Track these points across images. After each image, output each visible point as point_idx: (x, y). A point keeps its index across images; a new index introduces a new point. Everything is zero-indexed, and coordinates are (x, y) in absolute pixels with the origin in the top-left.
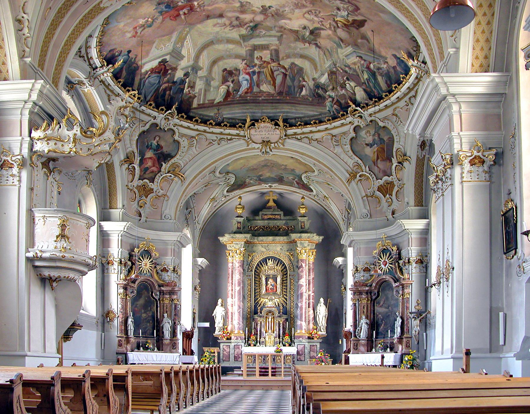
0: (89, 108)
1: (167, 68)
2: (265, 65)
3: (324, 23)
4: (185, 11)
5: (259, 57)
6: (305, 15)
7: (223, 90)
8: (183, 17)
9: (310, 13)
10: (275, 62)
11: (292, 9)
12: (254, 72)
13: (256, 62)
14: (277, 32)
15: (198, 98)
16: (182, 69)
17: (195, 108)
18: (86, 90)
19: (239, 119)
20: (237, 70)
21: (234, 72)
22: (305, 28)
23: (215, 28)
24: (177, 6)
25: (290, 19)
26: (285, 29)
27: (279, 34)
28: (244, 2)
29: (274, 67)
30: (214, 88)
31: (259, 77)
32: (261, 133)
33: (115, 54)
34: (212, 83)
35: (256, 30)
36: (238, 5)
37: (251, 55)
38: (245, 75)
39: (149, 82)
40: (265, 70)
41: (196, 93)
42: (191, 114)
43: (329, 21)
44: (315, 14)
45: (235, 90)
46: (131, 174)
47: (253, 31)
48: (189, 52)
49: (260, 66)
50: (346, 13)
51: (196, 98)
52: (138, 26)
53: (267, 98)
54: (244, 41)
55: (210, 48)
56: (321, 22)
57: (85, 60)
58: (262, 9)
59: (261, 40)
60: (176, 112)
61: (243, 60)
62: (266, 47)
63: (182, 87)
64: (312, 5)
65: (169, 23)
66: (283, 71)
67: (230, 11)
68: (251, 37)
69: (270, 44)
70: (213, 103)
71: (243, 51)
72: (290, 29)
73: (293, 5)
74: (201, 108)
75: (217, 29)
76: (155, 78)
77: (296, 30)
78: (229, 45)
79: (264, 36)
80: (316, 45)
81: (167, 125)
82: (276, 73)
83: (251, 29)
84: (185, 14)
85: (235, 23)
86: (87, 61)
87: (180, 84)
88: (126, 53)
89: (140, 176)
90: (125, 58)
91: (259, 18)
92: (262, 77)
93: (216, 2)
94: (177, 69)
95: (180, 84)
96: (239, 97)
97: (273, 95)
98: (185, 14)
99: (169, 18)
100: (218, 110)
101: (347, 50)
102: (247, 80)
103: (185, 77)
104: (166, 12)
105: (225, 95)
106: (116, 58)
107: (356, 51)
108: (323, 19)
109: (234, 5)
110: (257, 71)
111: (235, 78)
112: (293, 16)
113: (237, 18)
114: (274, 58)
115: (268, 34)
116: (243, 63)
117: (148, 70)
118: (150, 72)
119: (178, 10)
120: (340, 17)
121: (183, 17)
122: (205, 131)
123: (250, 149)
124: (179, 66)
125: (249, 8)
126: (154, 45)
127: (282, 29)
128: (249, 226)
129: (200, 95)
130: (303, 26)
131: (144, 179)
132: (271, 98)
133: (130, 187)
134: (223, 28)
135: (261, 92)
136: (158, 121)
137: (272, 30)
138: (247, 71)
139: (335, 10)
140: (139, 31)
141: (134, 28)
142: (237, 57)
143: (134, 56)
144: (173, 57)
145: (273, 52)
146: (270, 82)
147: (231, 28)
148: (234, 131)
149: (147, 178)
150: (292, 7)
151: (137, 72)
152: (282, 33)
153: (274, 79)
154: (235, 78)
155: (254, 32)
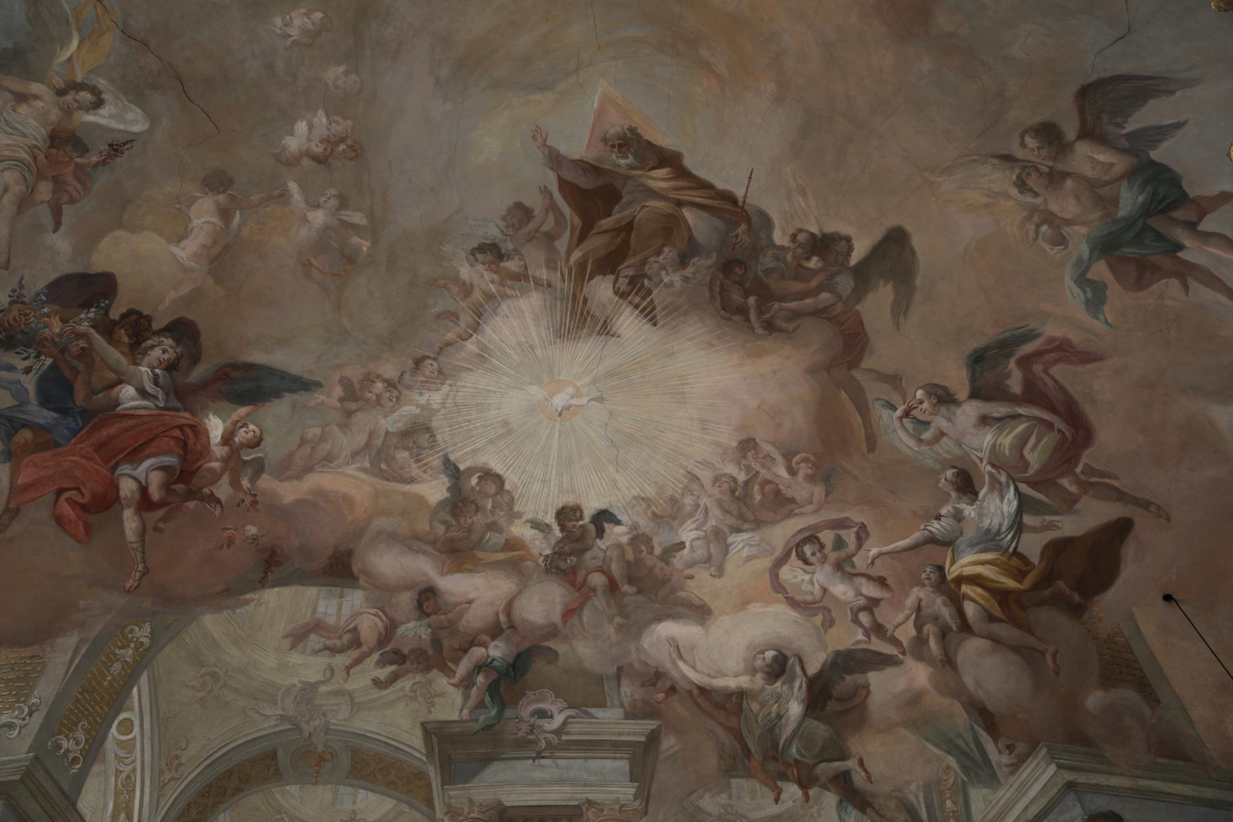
3: (883, 615)
6: (786, 573)
8: (130, 521)
9: (808, 550)
14: (631, 715)
22: (779, 668)
23: (295, 658)
24: (111, 410)
25: (701, 613)
26: (673, 689)
27: (637, 730)
28: (471, 471)
35: (515, 703)
36: (435, 490)
43: (916, 593)
44: (833, 556)
47: (503, 706)
50: (1009, 504)
54: (451, 775)
55: (254, 800)
56: (871, 605)
58: (558, 533)
64: (819, 491)
69: (589, 802)
72: (703, 690)
73: (720, 503)
78: (362, 793)
79: (562, 746)
80: (844, 785)
83: (493, 689)
84: (145, 503)
85: (414, 631)
101: (1022, 790)
107: (1081, 778)
108: (881, 582)
112: (718, 583)
113: (427, 597)
115: (579, 730)
120: (972, 545)
121: (130, 521)
125: (493, 527)
130: (770, 654)
134: (341, 660)
137: (601, 704)
139: (946, 499)
147: (383, 673)
152: (650, 725)
155: (509, 713)
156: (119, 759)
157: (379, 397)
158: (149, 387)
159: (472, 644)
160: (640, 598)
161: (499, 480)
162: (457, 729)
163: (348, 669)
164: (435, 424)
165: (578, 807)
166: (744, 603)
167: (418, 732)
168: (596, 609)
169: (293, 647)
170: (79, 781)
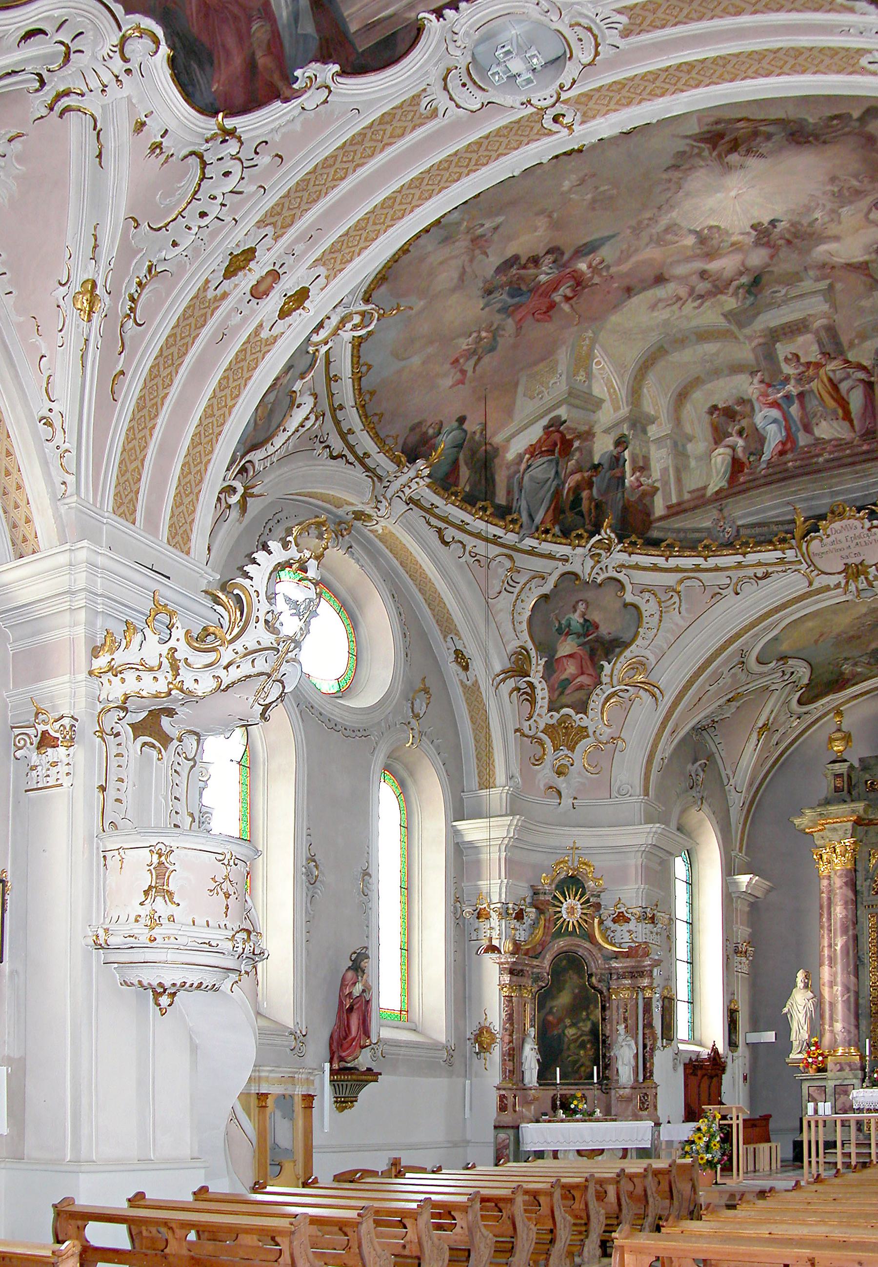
0: (400, 567)
1: (569, 437)
2: (811, 372)
4: (565, 290)
5: (790, 356)
7: (721, 457)
8: (566, 307)
10: (835, 358)
11: (833, 211)
12: (788, 397)
13: (788, 370)
14: (817, 280)
15: (663, 492)
16: (606, 431)
17: (662, 518)
18: (379, 528)
19: (777, 523)
20: (742, 401)
21: (738, 408)
23: (655, 314)
24: (539, 285)
25: (837, 238)
26: (833, 267)
27: (823, 285)
28: (702, 230)
29: (833, 371)
30: (699, 459)
31: (803, 406)
32: (838, 546)
33: (426, 433)
34: (689, 446)
35: (760, 291)
36: (690, 240)
37: (770, 356)
38: (767, 410)
39: (532, 478)
40: (814, 385)
41: (656, 481)
42: (655, 534)
45: (751, 454)
46: (527, 700)
47: (756, 296)
48: (610, 386)
49: (800, 379)
51: (659, 493)
52: (462, 356)
53: (836, 454)
54: (741, 325)
55: (661, 364)
57: (351, 464)
58: (754, 233)
59: (782, 312)
60: (613, 535)
61: (753, 374)
62: (801, 326)
63: (617, 472)
65: (536, 331)
66: (861, 375)
67: (679, 262)
68: (754, 311)
70: (703, 496)
71: (745, 352)
72: (849, 265)
74: (677, 513)
75: (662, 315)
76: (544, 466)
77: (861, 263)
78: (705, 345)
79: (786, 300)
81: (600, 572)
82: (844, 387)
83: (749, 292)
85: (703, 287)
86: (356, 463)
87: (612, 468)
88: (455, 424)
89: (551, 702)
90: (454, 436)
91: (758, 258)
92: (813, 404)
93: (633, 248)
94: (593, 435)
95: (612, 468)
96: (768, 468)
97: (849, 444)
98: (567, 299)
99: (530, 317)
100: (721, 510)
102: (775, 421)
103: (619, 449)
104: (518, 306)
105: (729, 469)
106: (432, 441)
109: (679, 244)
110: (795, 392)
111: (744, 423)
114: (829, 348)
116: (756, 380)
117: (521, 451)
118: (527, 456)
119: (547, 294)
122: (697, 569)
123: (819, 591)
124: (596, 427)
126: (521, 389)
127: (826, 268)
128: (866, 782)
129: (666, 483)
131: (562, 707)
132: (848, 452)
133: (526, 731)
134: (675, 307)
135: (818, 441)
136: (576, 568)
137: (801, 280)
138: (771, 398)
140: (469, 366)
141: (453, 363)
142: (736, 369)
143: (477, 428)
144: (577, 407)
145: (823, 333)
146: (835, 412)
147: (696, 304)
148: (771, 556)
149: (569, 703)
150: (829, 206)
151: (497, 461)
152: (828, 281)
153: (843, 403)
154: (744, 423)
155: (759, 297)
156: (601, 374)
157: (648, 225)
158: (550, 271)
159: (731, 281)
160: (805, 242)
161: (718, 227)
162: (737, 310)
163: (680, 308)
164: (678, 222)
165: (805, 318)
166: (857, 230)
167: (721, 317)
168: (784, 253)
169: (653, 310)
170: (590, 387)
